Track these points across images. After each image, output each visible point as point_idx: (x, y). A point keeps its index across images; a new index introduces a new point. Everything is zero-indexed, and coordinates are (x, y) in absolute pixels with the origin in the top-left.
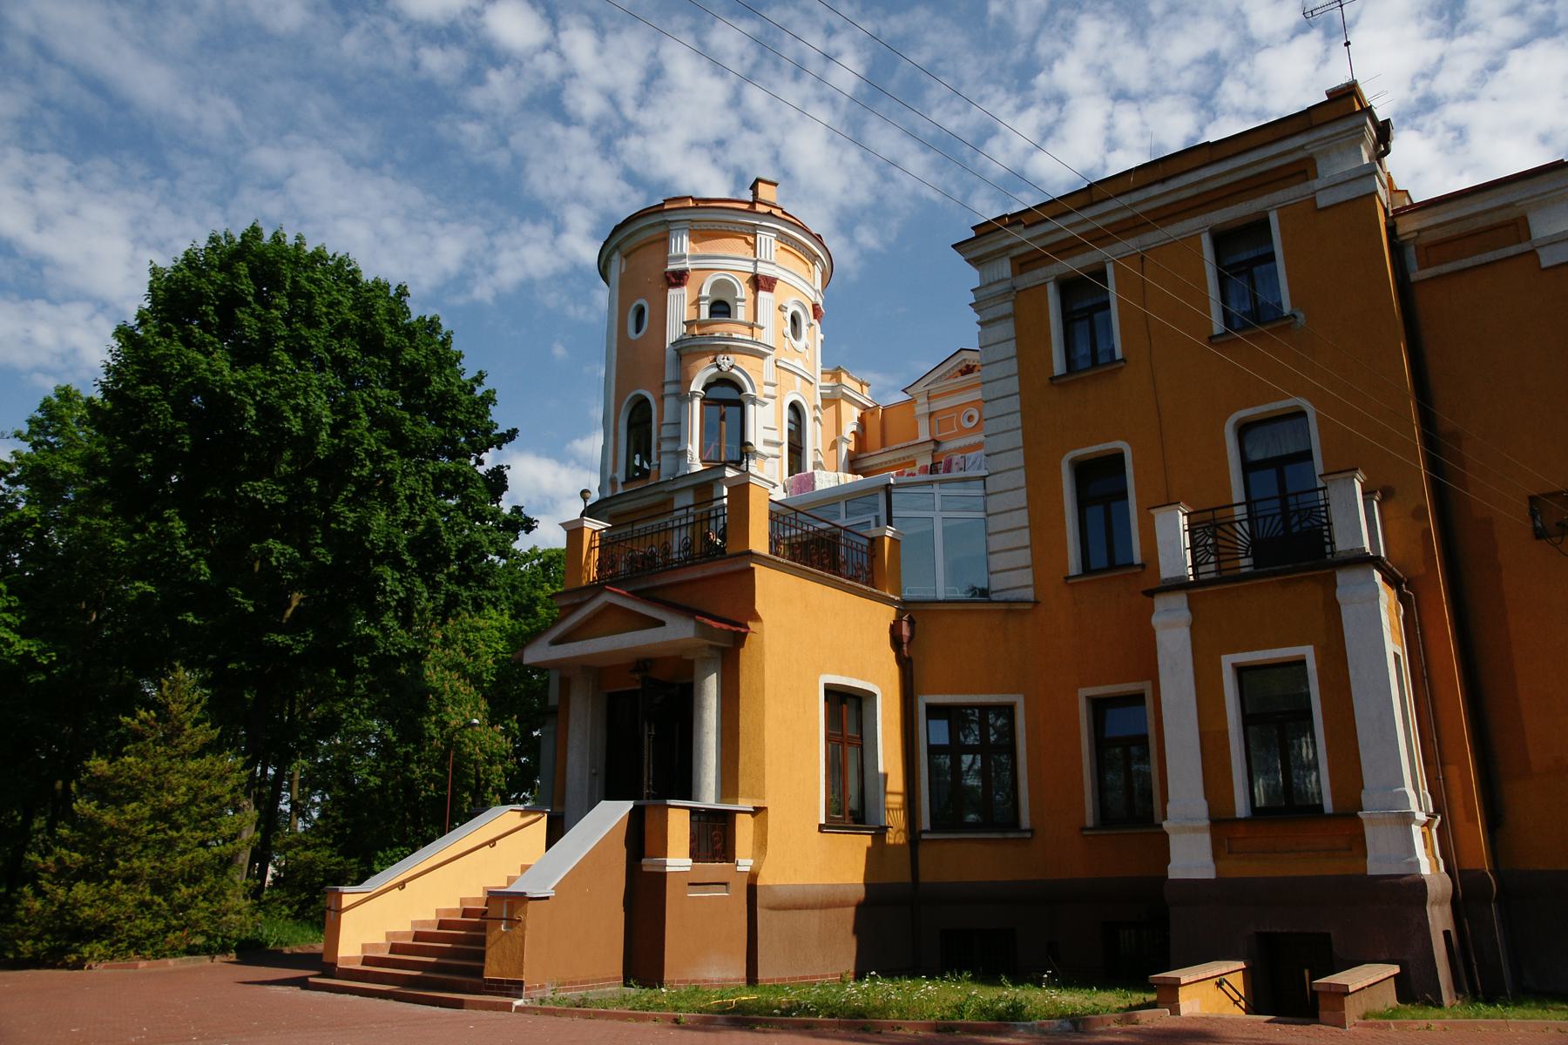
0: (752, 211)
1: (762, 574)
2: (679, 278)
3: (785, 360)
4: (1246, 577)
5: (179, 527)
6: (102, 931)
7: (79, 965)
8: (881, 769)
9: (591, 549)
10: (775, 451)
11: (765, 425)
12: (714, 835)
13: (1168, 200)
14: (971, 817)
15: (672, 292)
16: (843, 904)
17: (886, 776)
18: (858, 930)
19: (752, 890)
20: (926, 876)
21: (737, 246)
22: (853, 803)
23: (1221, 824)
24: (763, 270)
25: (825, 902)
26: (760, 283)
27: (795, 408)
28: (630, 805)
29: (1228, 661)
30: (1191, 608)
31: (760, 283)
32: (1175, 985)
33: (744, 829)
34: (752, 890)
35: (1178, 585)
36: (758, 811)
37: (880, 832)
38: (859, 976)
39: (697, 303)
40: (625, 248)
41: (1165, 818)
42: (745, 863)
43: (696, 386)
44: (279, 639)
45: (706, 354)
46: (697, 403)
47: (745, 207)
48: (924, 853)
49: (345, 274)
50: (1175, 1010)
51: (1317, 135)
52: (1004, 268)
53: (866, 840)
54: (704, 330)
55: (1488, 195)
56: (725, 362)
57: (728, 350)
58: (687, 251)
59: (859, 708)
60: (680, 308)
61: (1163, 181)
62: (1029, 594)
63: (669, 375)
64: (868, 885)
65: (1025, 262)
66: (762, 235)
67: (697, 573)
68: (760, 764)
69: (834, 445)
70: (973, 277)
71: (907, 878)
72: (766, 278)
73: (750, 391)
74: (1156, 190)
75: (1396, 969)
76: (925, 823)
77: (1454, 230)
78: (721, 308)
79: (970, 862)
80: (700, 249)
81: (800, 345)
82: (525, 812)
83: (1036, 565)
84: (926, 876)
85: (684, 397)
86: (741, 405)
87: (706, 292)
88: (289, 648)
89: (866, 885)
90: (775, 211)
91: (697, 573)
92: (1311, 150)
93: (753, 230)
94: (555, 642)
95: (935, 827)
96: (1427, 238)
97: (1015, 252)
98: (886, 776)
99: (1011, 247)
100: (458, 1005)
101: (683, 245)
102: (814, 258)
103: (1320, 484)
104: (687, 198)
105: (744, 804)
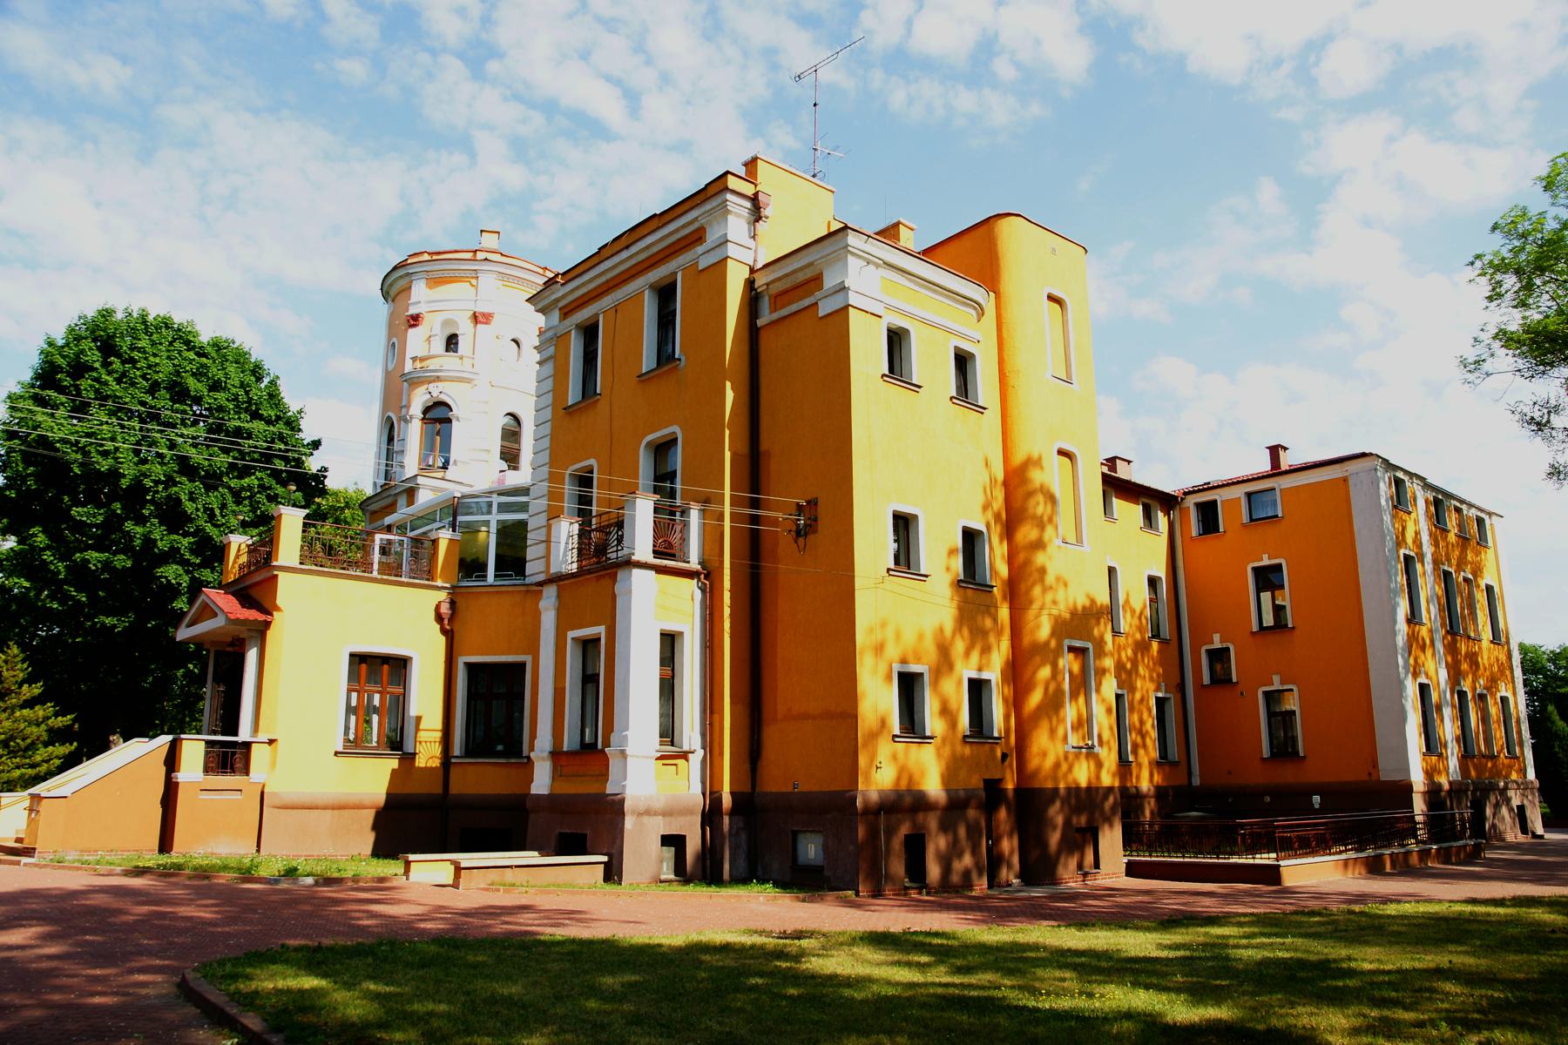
2: (415, 320)
4: (573, 575)
5: (41, 539)
9: (237, 557)
12: (229, 758)
13: (633, 262)
14: (500, 748)
15: (411, 331)
17: (419, 719)
18: (375, 827)
20: (456, 788)
23: (556, 755)
24: (481, 309)
29: (571, 634)
30: (559, 596)
33: (257, 753)
36: (271, 742)
37: (408, 758)
40: (392, 293)
41: (532, 748)
43: (416, 409)
44: (108, 621)
45: (422, 383)
47: (469, 255)
48: (454, 772)
49: (184, 338)
51: (708, 206)
52: (556, 315)
53: (394, 763)
54: (425, 364)
57: (438, 379)
61: (627, 247)
65: (566, 313)
67: (257, 578)
70: (540, 320)
71: (439, 790)
72: (483, 314)
74: (624, 255)
75: (605, 859)
76: (457, 749)
78: (452, 342)
79: (481, 779)
84: (456, 788)
86: (449, 421)
87: (437, 329)
88: (114, 626)
89: (388, 794)
90: (490, 256)
94: (189, 626)
95: (469, 751)
96: (775, 289)
97: (561, 304)
99: (557, 300)
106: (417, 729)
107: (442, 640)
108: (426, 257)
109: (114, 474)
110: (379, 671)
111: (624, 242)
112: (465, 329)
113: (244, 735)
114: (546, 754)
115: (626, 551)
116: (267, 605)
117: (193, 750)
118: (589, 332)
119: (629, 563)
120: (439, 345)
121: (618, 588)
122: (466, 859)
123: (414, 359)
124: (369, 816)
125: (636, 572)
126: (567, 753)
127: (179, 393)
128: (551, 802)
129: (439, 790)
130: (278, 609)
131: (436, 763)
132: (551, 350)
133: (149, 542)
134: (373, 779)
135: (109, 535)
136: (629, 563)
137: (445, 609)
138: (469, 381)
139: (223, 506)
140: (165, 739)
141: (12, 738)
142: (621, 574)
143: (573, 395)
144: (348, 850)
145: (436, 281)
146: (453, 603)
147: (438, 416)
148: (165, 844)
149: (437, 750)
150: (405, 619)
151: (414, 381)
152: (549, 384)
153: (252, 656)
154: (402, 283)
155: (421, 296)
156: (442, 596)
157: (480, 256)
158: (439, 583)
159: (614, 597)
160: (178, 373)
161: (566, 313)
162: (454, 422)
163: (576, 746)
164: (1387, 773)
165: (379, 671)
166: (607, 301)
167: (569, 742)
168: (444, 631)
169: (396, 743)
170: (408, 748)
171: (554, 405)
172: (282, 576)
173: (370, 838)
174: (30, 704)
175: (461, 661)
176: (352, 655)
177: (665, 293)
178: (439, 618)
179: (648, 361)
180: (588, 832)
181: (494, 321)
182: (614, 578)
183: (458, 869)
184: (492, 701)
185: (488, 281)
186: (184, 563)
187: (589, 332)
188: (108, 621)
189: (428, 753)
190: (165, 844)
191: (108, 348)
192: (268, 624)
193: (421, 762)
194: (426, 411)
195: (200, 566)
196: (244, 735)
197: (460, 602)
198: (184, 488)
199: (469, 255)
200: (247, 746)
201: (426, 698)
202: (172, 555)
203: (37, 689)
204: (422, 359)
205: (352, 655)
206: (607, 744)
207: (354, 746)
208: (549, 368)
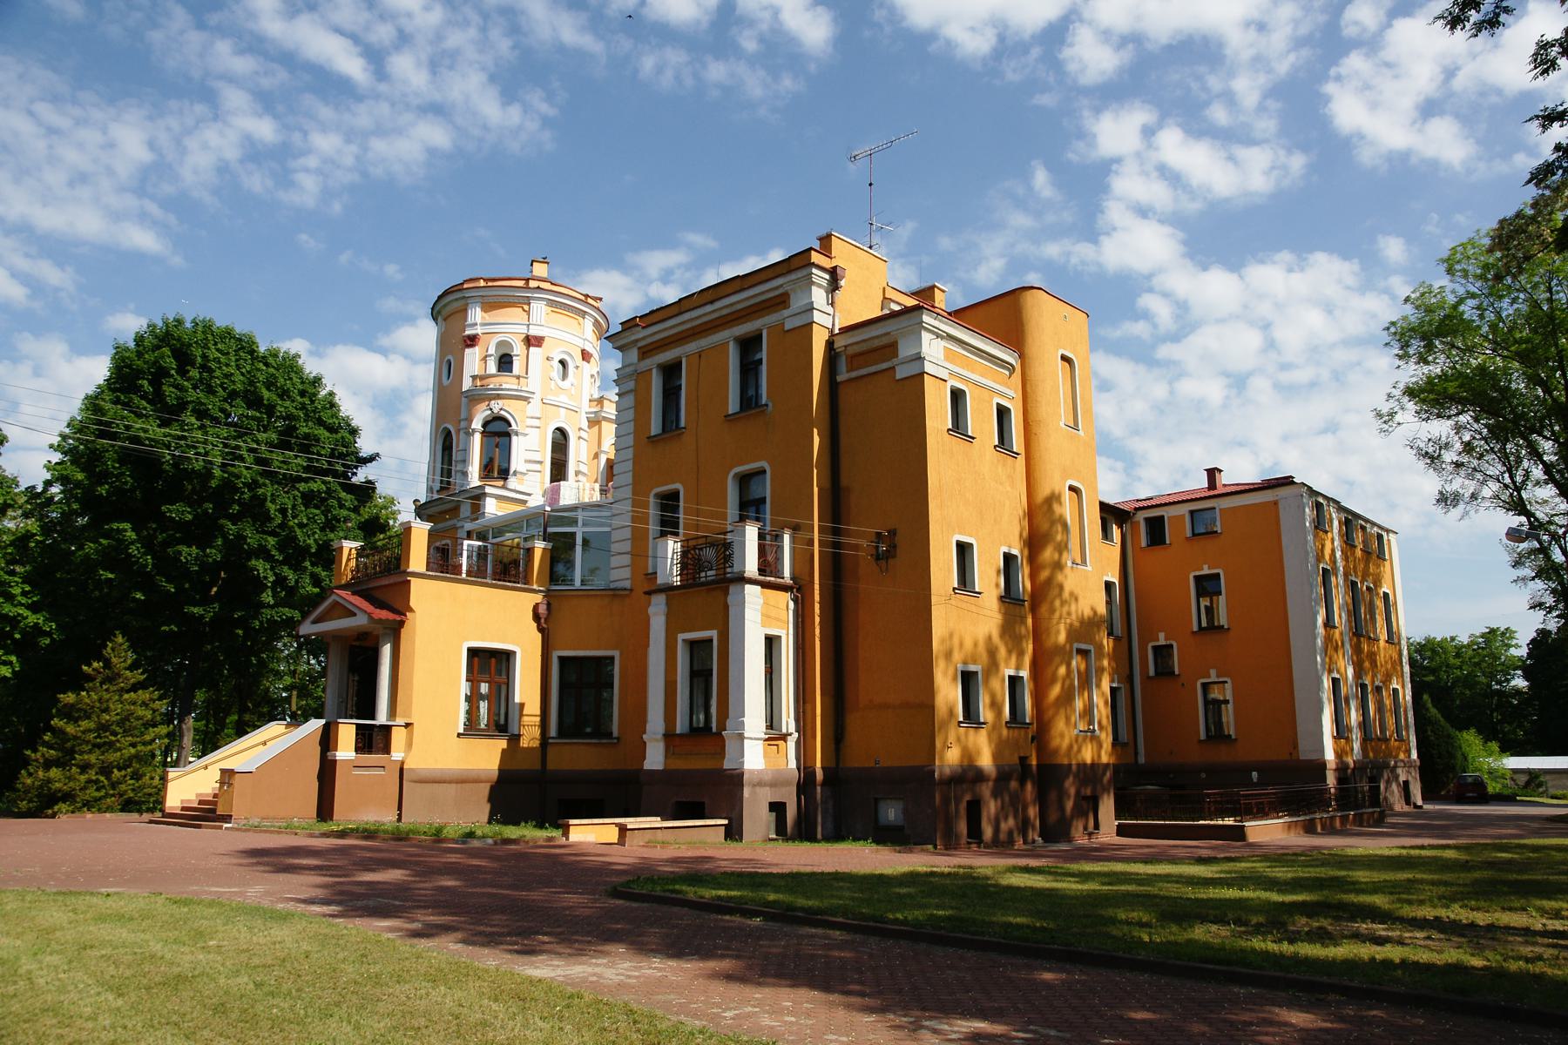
0: (527, 288)
1: (415, 584)
2: (472, 341)
3: (550, 398)
6: (68, 797)
7: (53, 816)
8: (517, 700)
9: (349, 560)
10: (537, 467)
11: (529, 450)
12: (373, 740)
14: (588, 730)
15: (468, 351)
16: (477, 781)
17: (522, 705)
18: (490, 800)
19: (402, 770)
20: (551, 766)
21: (515, 314)
22: (502, 721)
23: (669, 736)
24: (534, 331)
25: (463, 780)
26: (531, 341)
27: (561, 433)
28: (323, 722)
29: (681, 637)
31: (531, 341)
32: (568, 826)
33: (398, 736)
34: (402, 770)
35: (668, 589)
36: (407, 725)
37: (514, 739)
38: (489, 822)
39: (484, 359)
40: (445, 312)
42: (397, 754)
43: (477, 424)
45: (483, 400)
46: (477, 438)
47: (521, 283)
48: (551, 752)
49: (246, 346)
50: (566, 834)
51: (793, 276)
52: (634, 355)
53: (502, 744)
55: (873, 327)
56: (497, 406)
57: (499, 397)
58: (479, 321)
59: (508, 660)
60: (474, 362)
62: (627, 584)
63: (463, 416)
64: (502, 771)
65: (645, 353)
66: (534, 304)
67: (385, 582)
68: (410, 697)
69: (596, 456)
71: (538, 766)
72: (536, 338)
73: (514, 427)
74: (709, 308)
75: (725, 822)
76: (553, 732)
77: (864, 347)
78: (505, 362)
79: (578, 757)
80: (489, 317)
81: (566, 384)
82: (288, 725)
83: (633, 566)
84: (551, 766)
85: (469, 433)
86: (508, 435)
87: (492, 350)
91: (385, 582)
92: (787, 288)
93: (528, 301)
94: (314, 622)
95: (562, 733)
96: (851, 351)
98: (522, 705)
99: (637, 341)
100: (199, 827)
101: (476, 315)
102: (583, 314)
103: (729, 528)
104: (477, 279)
105: (400, 721)
106: (521, 715)
107: (537, 637)
108: (482, 283)
109: (207, 474)
110: (489, 665)
111: (708, 296)
112: (518, 349)
113: (382, 718)
114: (660, 736)
115: (736, 569)
116: (397, 606)
117: (347, 733)
118: (671, 372)
119: (743, 580)
120: (492, 368)
121: (730, 599)
122: (631, 822)
123: (474, 377)
124: (485, 790)
125: (747, 587)
126: (681, 735)
127: (254, 401)
128: (663, 777)
129: (538, 766)
130: (411, 610)
131: (536, 744)
132: (631, 385)
133: (241, 538)
134: (487, 756)
135: (201, 532)
136: (743, 580)
137: (542, 610)
138: (526, 399)
139: (294, 507)
140: (315, 724)
141: (127, 719)
142: (732, 589)
143: (655, 427)
144: (472, 815)
145: (489, 306)
146: (549, 605)
147: (499, 432)
148: (325, 809)
149: (537, 732)
150: (508, 619)
151: (475, 397)
152: (630, 414)
153: (386, 651)
154: (456, 305)
155: (476, 316)
156: (539, 598)
157: (533, 284)
158: (535, 587)
159: (726, 607)
160: (252, 383)
161: (645, 353)
162: (514, 439)
163: (686, 729)
164: (1305, 754)
165: (489, 665)
166: (692, 347)
167: (681, 726)
168: (540, 629)
169: (502, 725)
170: (514, 729)
171: (636, 432)
172: (414, 581)
173: (487, 808)
174: (134, 688)
175: (556, 654)
176: (473, 652)
177: (749, 345)
178: (536, 617)
179: (733, 405)
180: (706, 800)
181: (545, 344)
182: (726, 592)
183: (623, 830)
184: (581, 687)
185: (539, 309)
186: (268, 557)
187: (671, 372)
188: (196, 610)
189: (530, 735)
190: (325, 809)
191: (183, 357)
192: (402, 624)
193: (524, 743)
194: (484, 426)
195: (283, 563)
196: (382, 718)
197: (555, 604)
198: (268, 489)
199: (521, 283)
200: (387, 729)
201: (526, 687)
202: (263, 552)
203: (138, 676)
204: (482, 378)
205: (473, 652)
206: (722, 726)
207: (472, 728)
208: (630, 400)
